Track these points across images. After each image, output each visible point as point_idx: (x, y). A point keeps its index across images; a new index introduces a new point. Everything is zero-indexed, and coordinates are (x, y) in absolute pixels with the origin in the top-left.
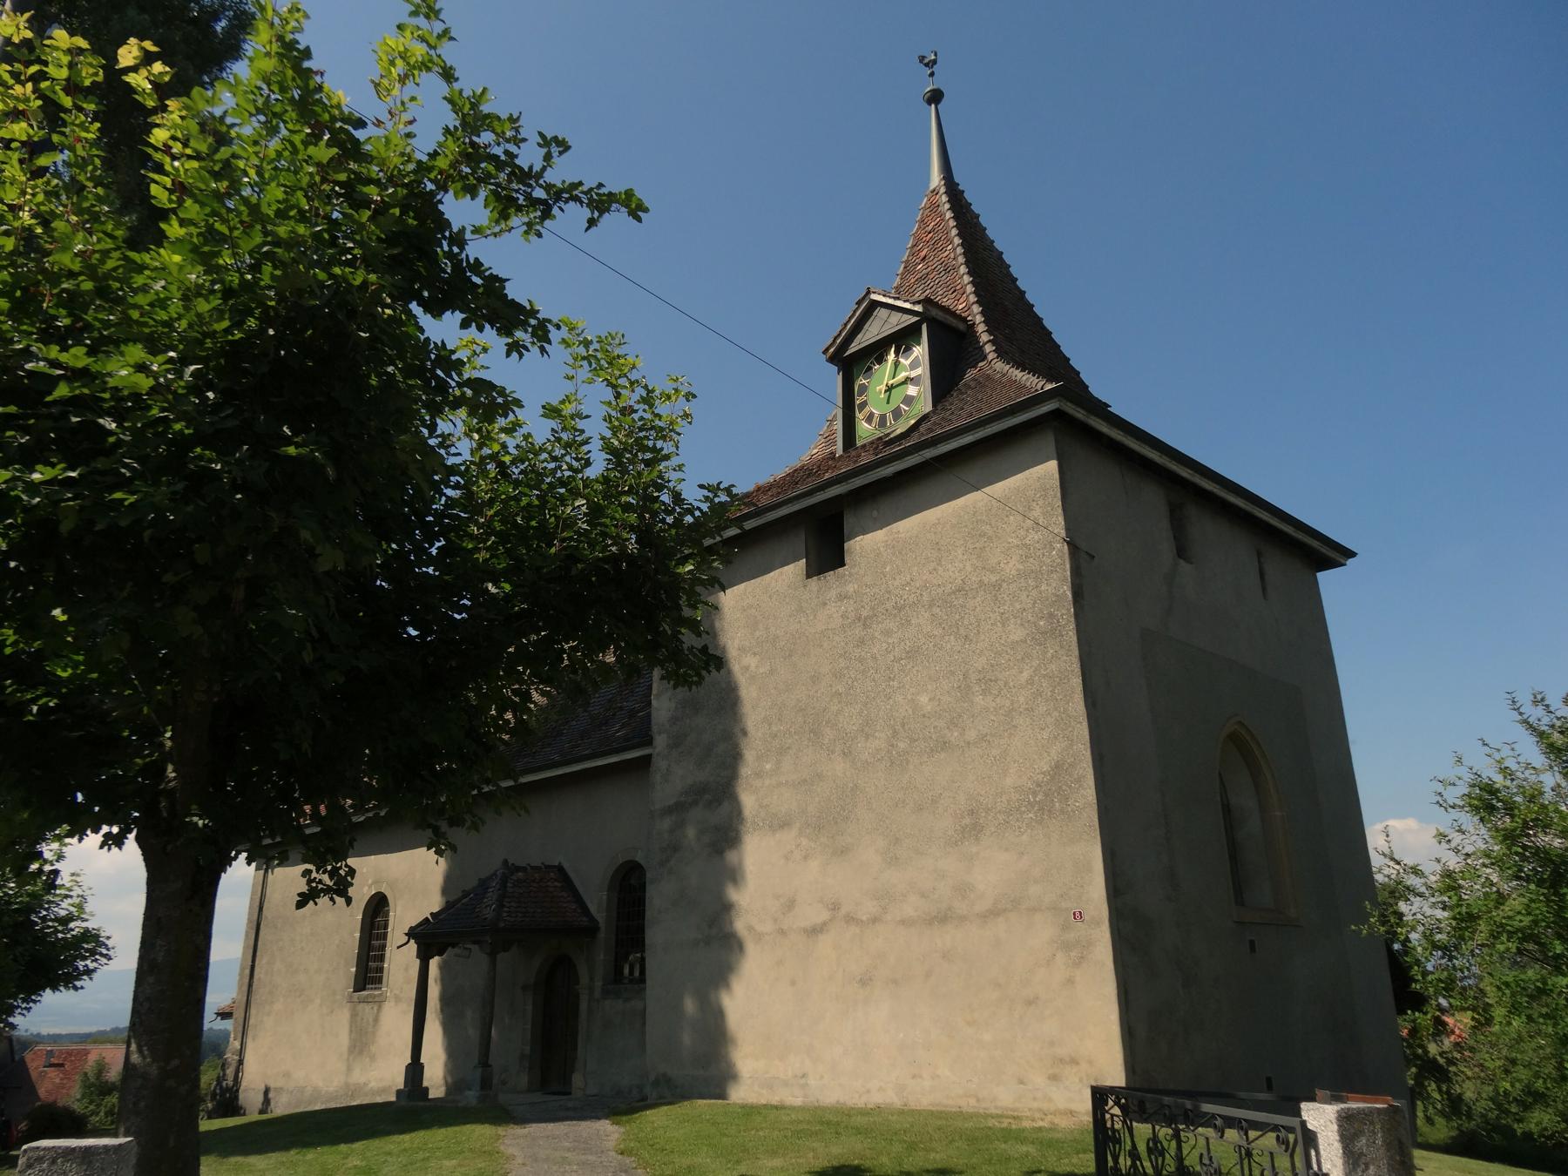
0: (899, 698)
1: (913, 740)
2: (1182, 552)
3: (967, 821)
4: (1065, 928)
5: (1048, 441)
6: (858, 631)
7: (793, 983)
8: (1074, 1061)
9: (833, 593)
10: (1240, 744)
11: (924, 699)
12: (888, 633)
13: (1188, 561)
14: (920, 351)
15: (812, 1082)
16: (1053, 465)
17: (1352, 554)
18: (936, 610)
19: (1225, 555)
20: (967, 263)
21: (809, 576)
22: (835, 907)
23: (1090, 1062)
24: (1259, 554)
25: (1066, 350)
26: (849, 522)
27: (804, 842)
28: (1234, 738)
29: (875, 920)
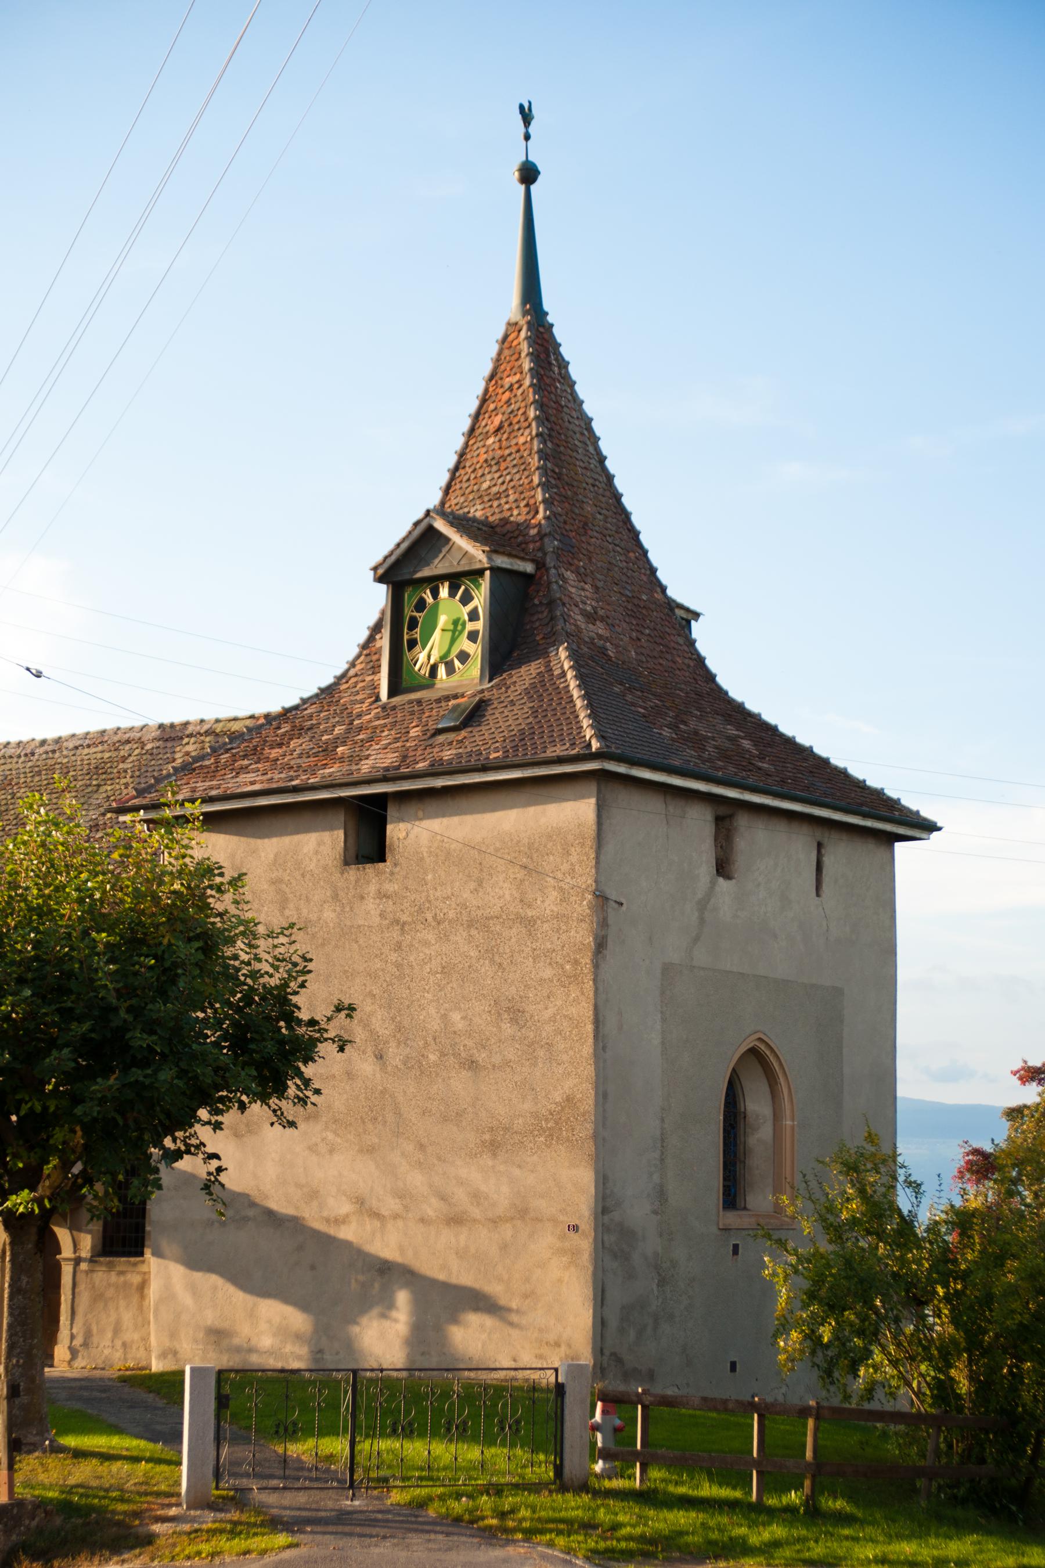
0: (432, 1011)
1: (443, 1054)
2: (723, 868)
3: (487, 1137)
4: (562, 1237)
5: (593, 787)
6: (395, 934)
7: (313, 1268)
8: (557, 1344)
9: (372, 888)
10: (758, 1057)
11: (456, 1017)
12: (426, 943)
13: (728, 877)
14: (481, 597)
15: (327, 1356)
16: (593, 801)
17: (930, 827)
18: (474, 932)
19: (776, 857)
20: (545, 486)
21: (346, 863)
22: (360, 1202)
23: (569, 1346)
24: (820, 846)
25: (655, 558)
26: (392, 812)
27: (330, 1136)
28: (753, 1051)
29: (396, 1217)
